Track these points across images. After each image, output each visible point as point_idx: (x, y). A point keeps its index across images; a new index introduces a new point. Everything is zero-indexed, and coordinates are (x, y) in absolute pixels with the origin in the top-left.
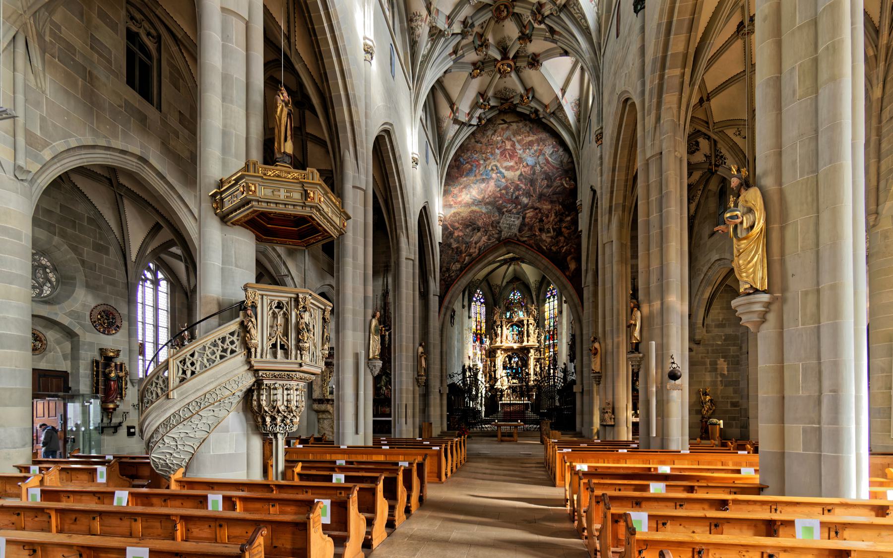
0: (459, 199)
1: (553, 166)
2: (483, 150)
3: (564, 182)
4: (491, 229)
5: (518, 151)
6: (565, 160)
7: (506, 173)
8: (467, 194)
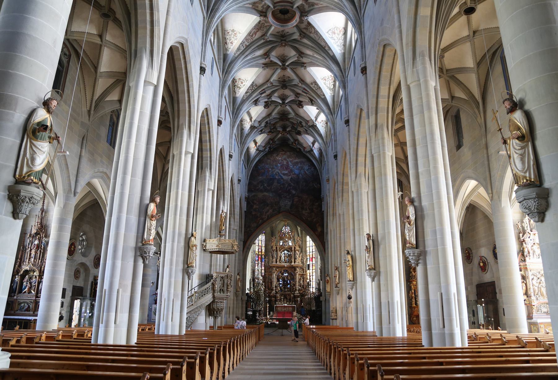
0: (258, 188)
4: (274, 205)
5: (290, 166)
7: (284, 177)
8: (261, 185)
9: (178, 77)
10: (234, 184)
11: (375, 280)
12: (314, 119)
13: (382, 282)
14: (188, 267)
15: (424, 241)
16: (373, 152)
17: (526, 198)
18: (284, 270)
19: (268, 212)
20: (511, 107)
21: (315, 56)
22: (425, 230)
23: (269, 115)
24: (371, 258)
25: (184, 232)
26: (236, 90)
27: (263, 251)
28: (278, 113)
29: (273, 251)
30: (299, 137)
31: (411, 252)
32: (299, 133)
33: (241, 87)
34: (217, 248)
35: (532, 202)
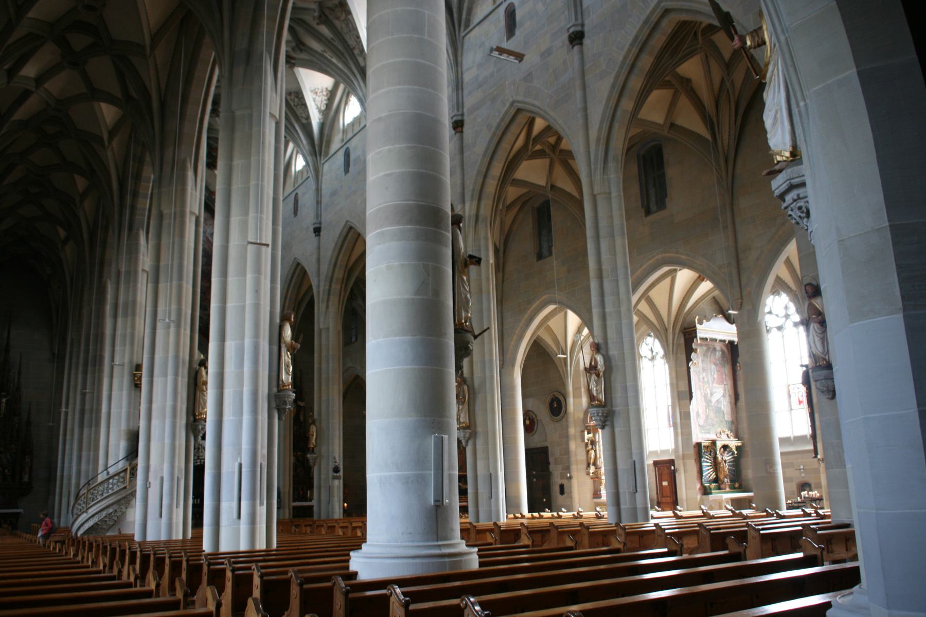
14: (195, 420)
21: (327, 55)
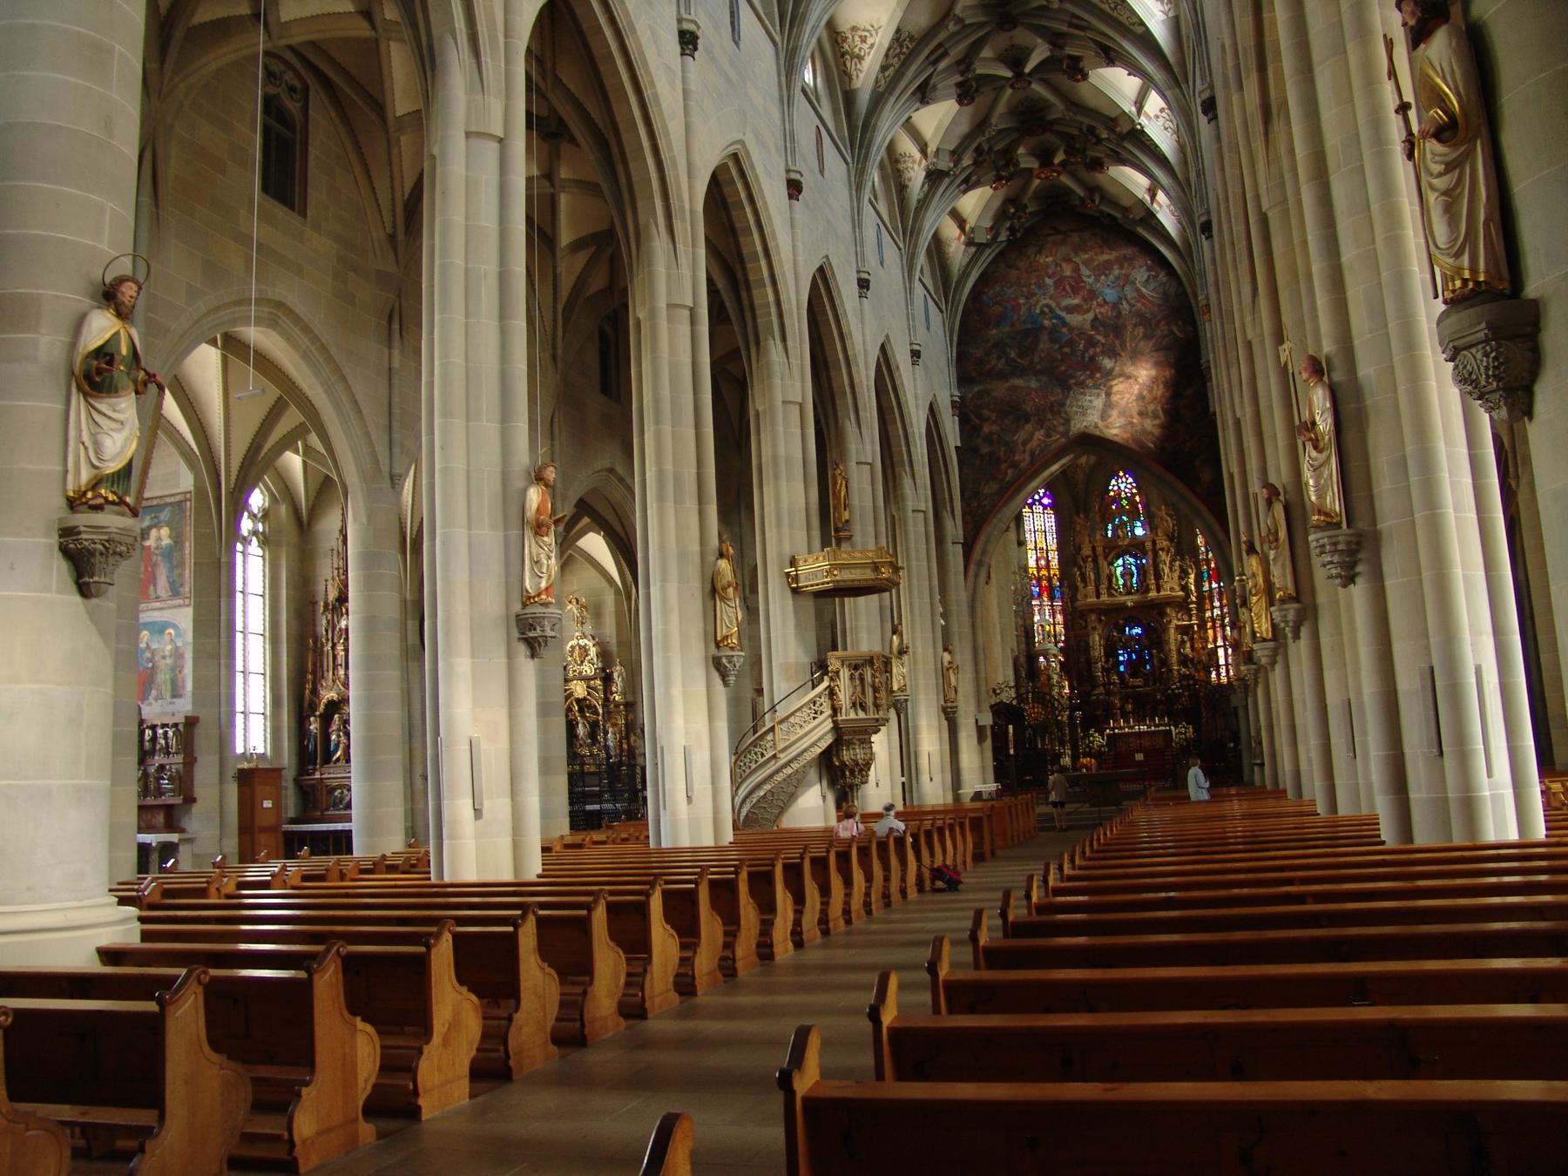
0: (988, 367)
1: (1152, 302)
2: (1023, 282)
3: (1175, 329)
4: (1049, 416)
5: (1085, 279)
6: (1172, 291)
7: (1069, 318)
8: (999, 358)
9: (608, 82)
10: (898, 367)
11: (1302, 634)
12: (1130, 108)
13: (1325, 640)
15: (1371, 498)
16: (1265, 206)
17: (1458, 343)
18: (1125, 619)
19: (1031, 440)
20: (1419, 21)
22: (1372, 462)
23: (980, 125)
24: (1283, 566)
25: (695, 547)
26: (848, 65)
27: (1055, 563)
28: (1013, 111)
29: (1085, 561)
30: (1100, 177)
31: (1326, 540)
32: (1097, 165)
33: (862, 54)
34: (828, 579)
35: (1479, 356)
